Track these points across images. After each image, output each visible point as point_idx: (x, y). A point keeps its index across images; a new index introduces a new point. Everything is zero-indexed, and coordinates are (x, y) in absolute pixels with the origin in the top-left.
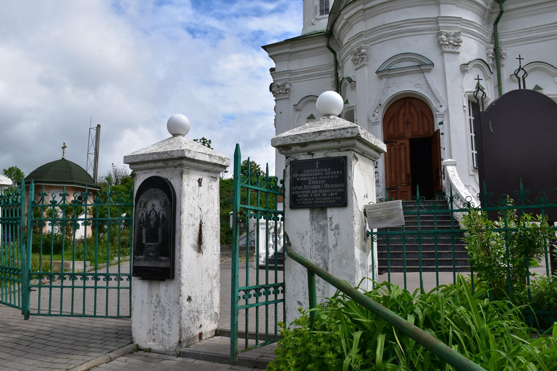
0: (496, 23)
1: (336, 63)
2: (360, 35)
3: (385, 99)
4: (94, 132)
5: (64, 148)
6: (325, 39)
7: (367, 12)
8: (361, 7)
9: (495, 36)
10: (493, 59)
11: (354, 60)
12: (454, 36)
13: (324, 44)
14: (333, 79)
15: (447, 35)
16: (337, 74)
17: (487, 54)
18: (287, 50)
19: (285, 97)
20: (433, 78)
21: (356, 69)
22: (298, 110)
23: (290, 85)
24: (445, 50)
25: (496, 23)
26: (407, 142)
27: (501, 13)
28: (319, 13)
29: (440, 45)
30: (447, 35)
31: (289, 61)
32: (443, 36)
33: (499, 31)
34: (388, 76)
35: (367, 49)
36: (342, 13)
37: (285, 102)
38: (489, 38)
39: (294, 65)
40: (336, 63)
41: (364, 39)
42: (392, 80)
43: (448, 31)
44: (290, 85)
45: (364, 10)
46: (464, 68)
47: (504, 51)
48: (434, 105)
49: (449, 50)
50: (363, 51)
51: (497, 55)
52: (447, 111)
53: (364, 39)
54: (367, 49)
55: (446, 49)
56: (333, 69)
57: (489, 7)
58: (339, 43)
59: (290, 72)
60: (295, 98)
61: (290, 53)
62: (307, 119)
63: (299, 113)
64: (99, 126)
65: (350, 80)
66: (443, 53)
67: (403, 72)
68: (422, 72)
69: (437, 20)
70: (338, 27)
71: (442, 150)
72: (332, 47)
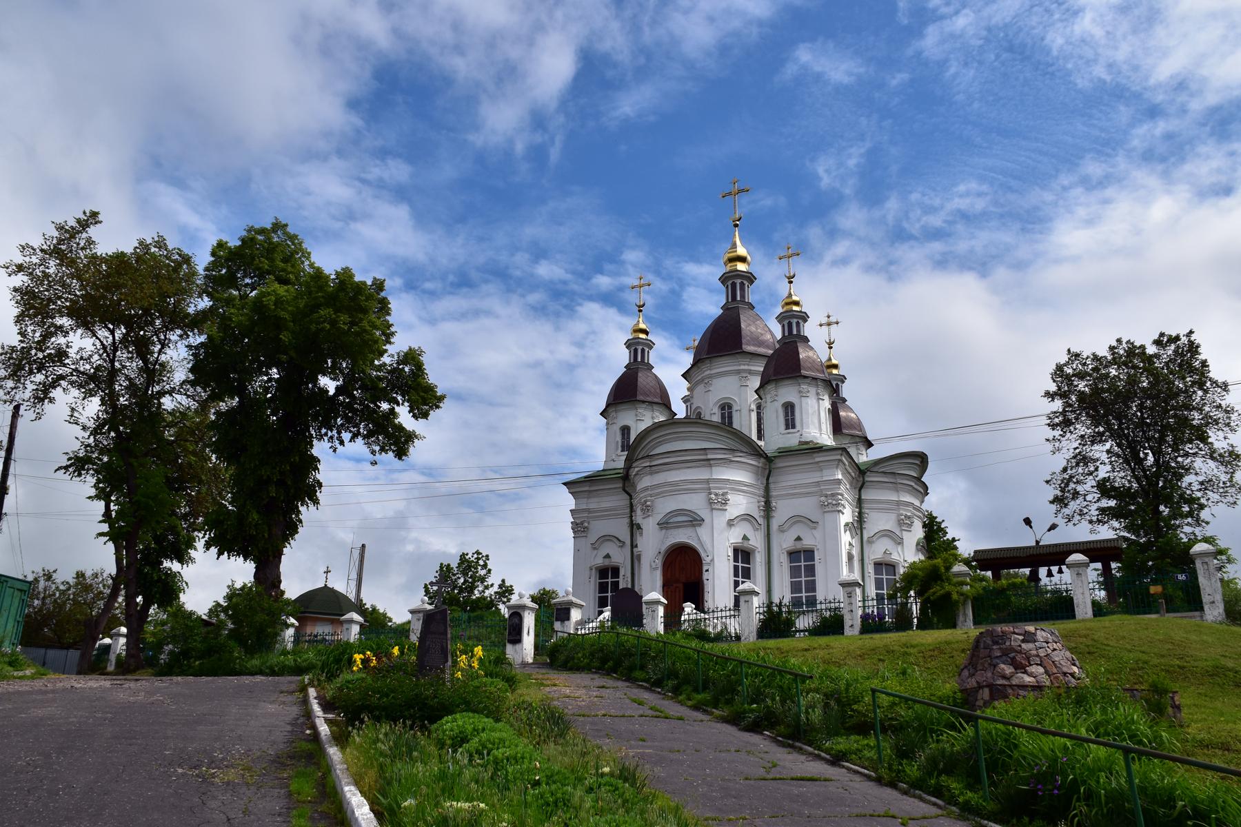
0: (768, 479)
1: (631, 506)
2: (646, 489)
3: (664, 548)
4: (356, 554)
5: (327, 572)
6: (621, 481)
7: (654, 468)
8: (648, 464)
9: (767, 489)
10: (764, 511)
11: (642, 510)
12: (722, 495)
13: (621, 485)
14: (627, 520)
15: (716, 495)
16: (631, 516)
17: (759, 507)
18: (587, 488)
19: (583, 535)
20: (703, 531)
21: (644, 518)
22: (595, 549)
23: (589, 523)
24: (714, 507)
25: (768, 479)
26: (681, 586)
27: (770, 472)
28: (620, 449)
29: (710, 502)
30: (716, 495)
31: (588, 498)
32: (713, 496)
33: (772, 486)
34: (667, 528)
35: (652, 501)
36: (634, 465)
37: (583, 539)
38: (762, 492)
39: (594, 504)
40: (631, 506)
41: (649, 492)
42: (670, 532)
43: (717, 491)
44: (589, 523)
45: (650, 466)
46: (730, 523)
47: (774, 504)
48: (703, 555)
49: (717, 507)
50: (648, 503)
51: (768, 509)
52: (712, 560)
53: (649, 492)
54: (652, 501)
55: (715, 506)
56: (628, 510)
57: (760, 465)
58: (634, 486)
59: (588, 511)
60: (593, 537)
61: (590, 491)
62: (605, 557)
63: (596, 551)
64: (363, 546)
65: (639, 527)
66: (712, 509)
67: (679, 526)
68: (694, 526)
69: (708, 481)
70: (633, 472)
71: (706, 594)
72: (627, 489)
